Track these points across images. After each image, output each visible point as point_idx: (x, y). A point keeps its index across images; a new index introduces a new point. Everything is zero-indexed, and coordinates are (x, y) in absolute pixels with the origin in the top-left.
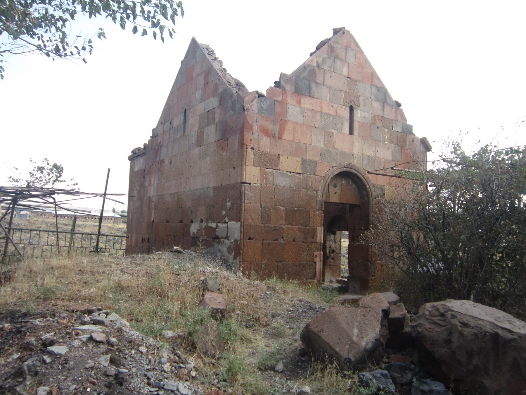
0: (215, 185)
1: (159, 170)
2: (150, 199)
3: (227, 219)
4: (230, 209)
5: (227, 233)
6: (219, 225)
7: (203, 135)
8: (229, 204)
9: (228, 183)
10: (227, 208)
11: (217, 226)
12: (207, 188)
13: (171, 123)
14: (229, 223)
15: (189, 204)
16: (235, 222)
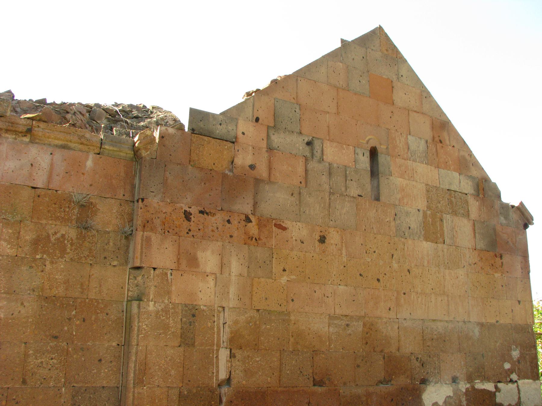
0: (484, 321)
1: (251, 240)
2: (192, 313)
3: (514, 377)
4: (518, 361)
5: (519, 398)
6: (500, 385)
7: (442, 226)
8: (516, 354)
9: (511, 322)
10: (512, 359)
11: (496, 387)
12: (464, 322)
13: (309, 144)
14: (520, 382)
15: (410, 346)
16: (531, 381)
